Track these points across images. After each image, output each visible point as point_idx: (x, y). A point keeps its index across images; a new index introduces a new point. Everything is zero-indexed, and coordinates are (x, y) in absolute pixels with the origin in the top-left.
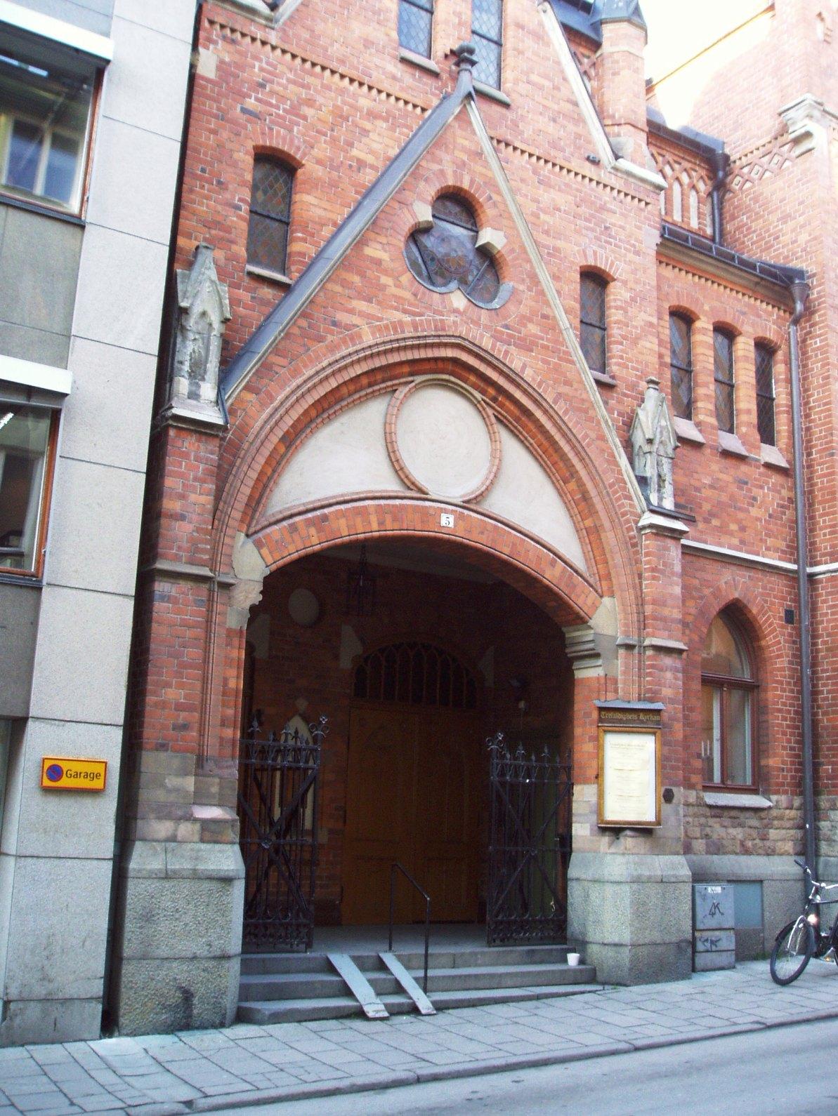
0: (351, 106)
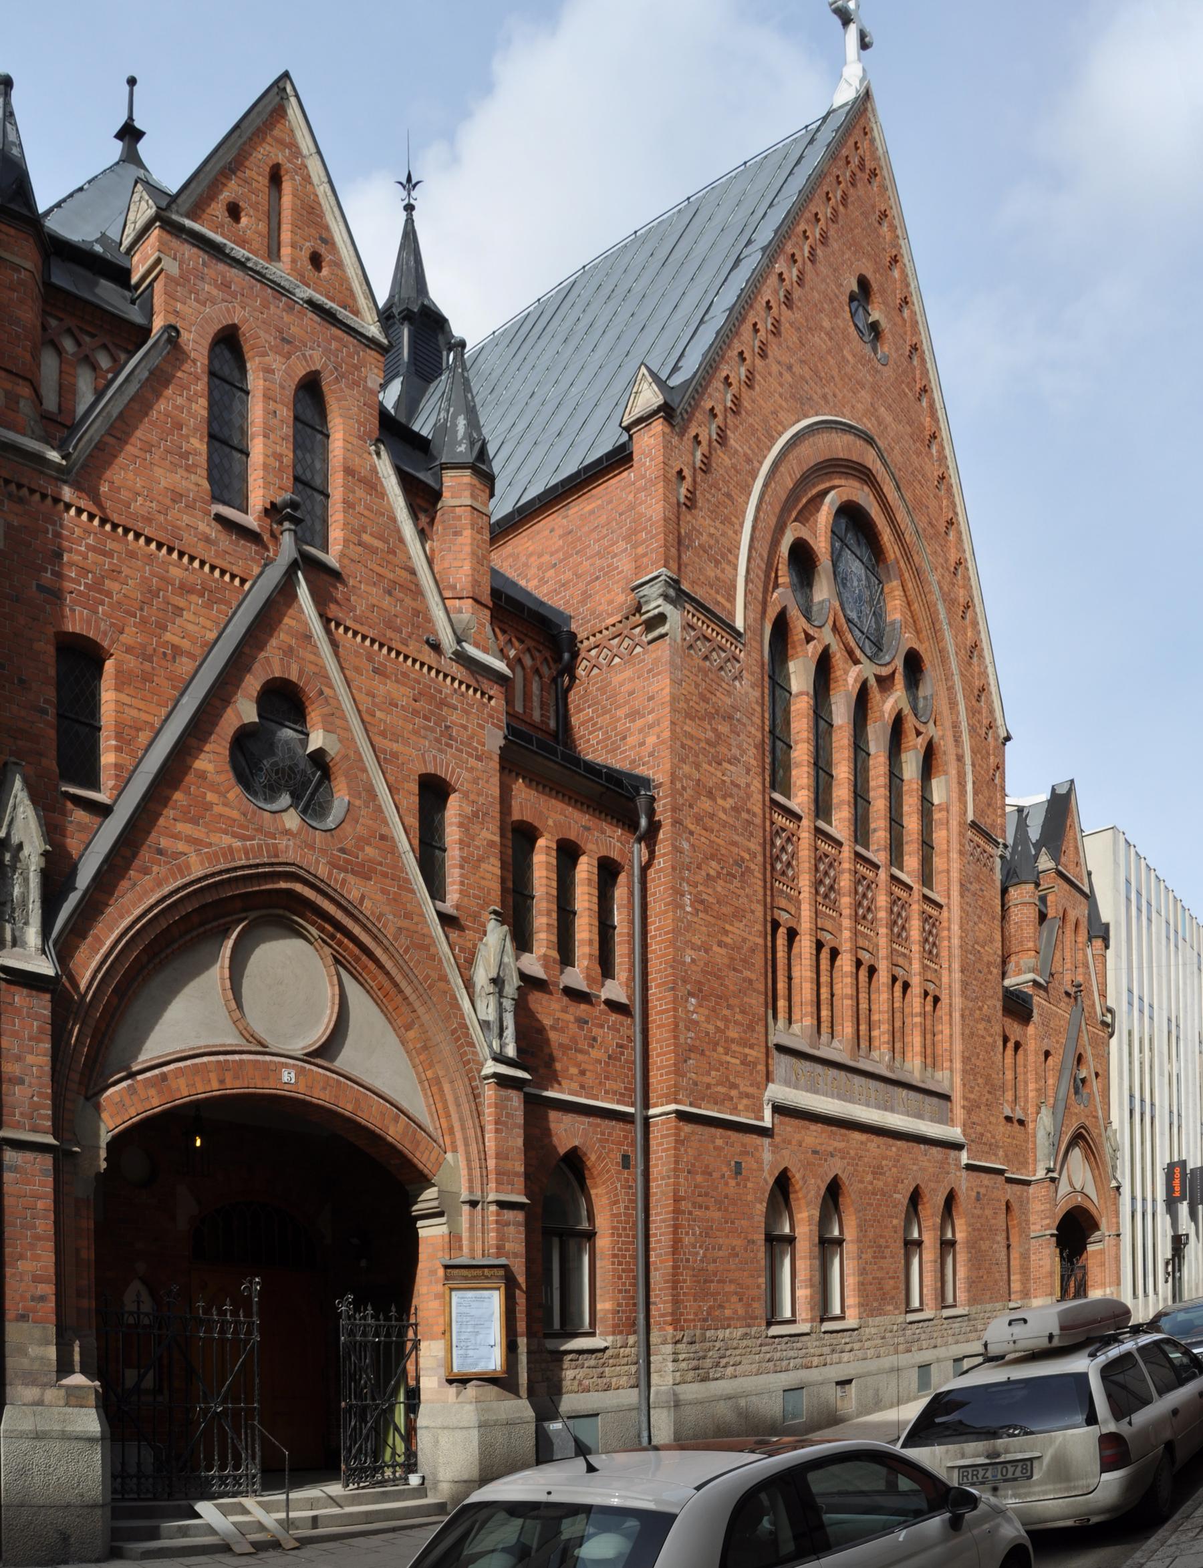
0: (162, 578)
